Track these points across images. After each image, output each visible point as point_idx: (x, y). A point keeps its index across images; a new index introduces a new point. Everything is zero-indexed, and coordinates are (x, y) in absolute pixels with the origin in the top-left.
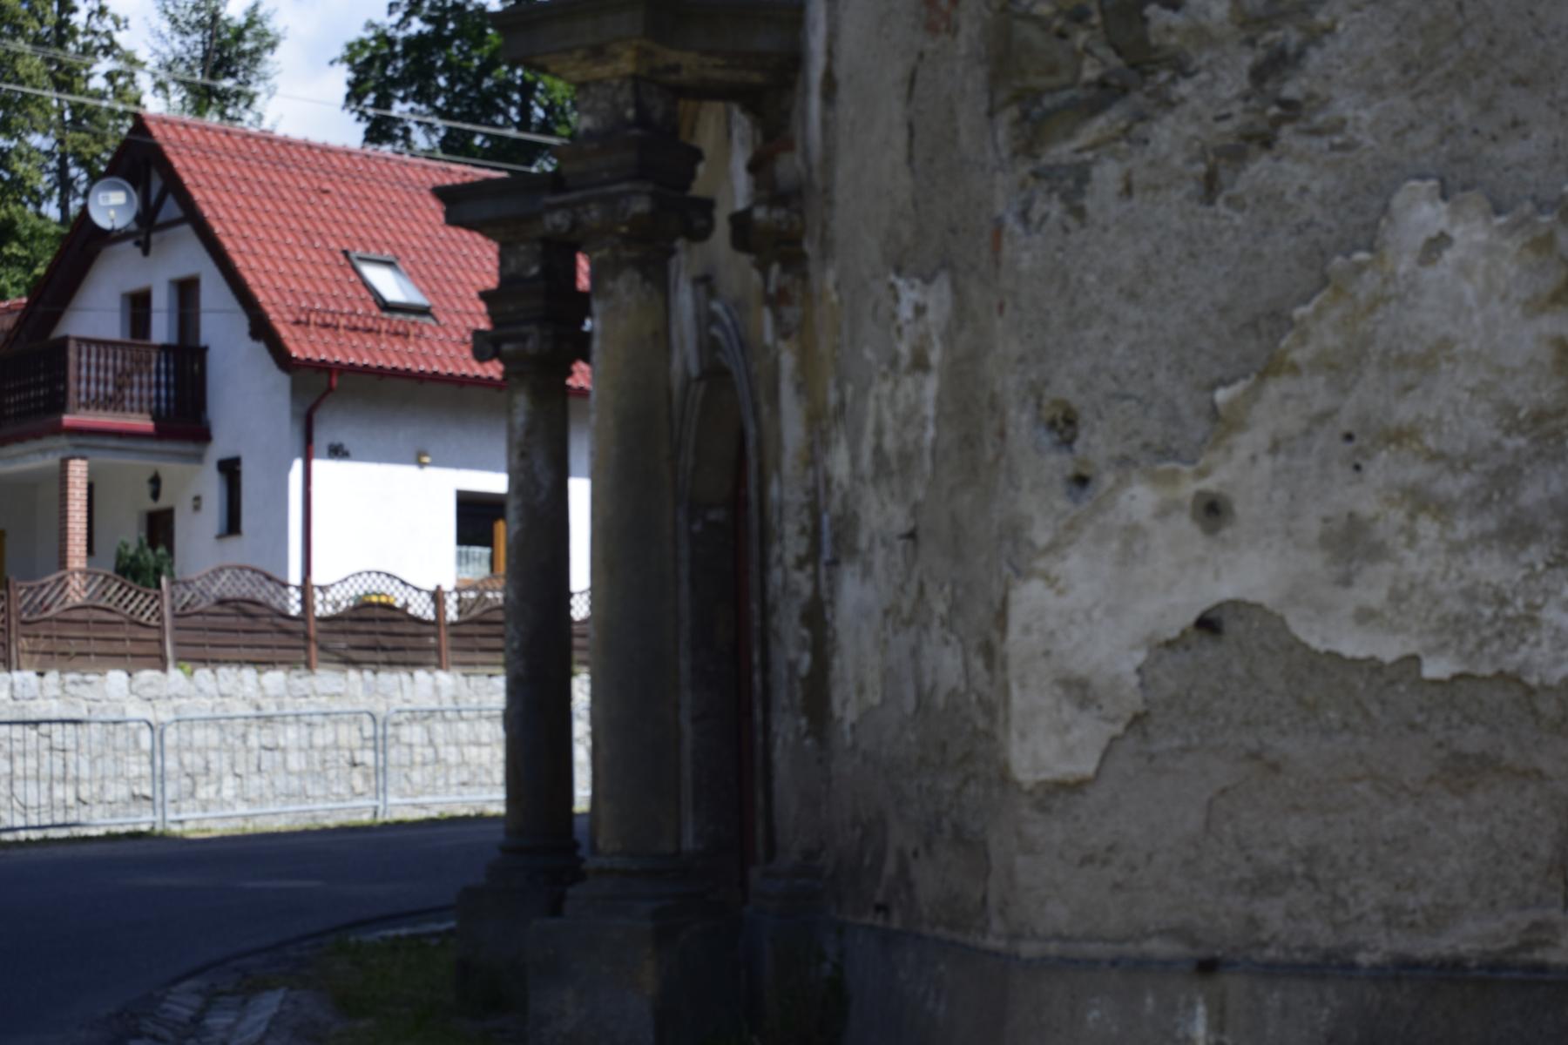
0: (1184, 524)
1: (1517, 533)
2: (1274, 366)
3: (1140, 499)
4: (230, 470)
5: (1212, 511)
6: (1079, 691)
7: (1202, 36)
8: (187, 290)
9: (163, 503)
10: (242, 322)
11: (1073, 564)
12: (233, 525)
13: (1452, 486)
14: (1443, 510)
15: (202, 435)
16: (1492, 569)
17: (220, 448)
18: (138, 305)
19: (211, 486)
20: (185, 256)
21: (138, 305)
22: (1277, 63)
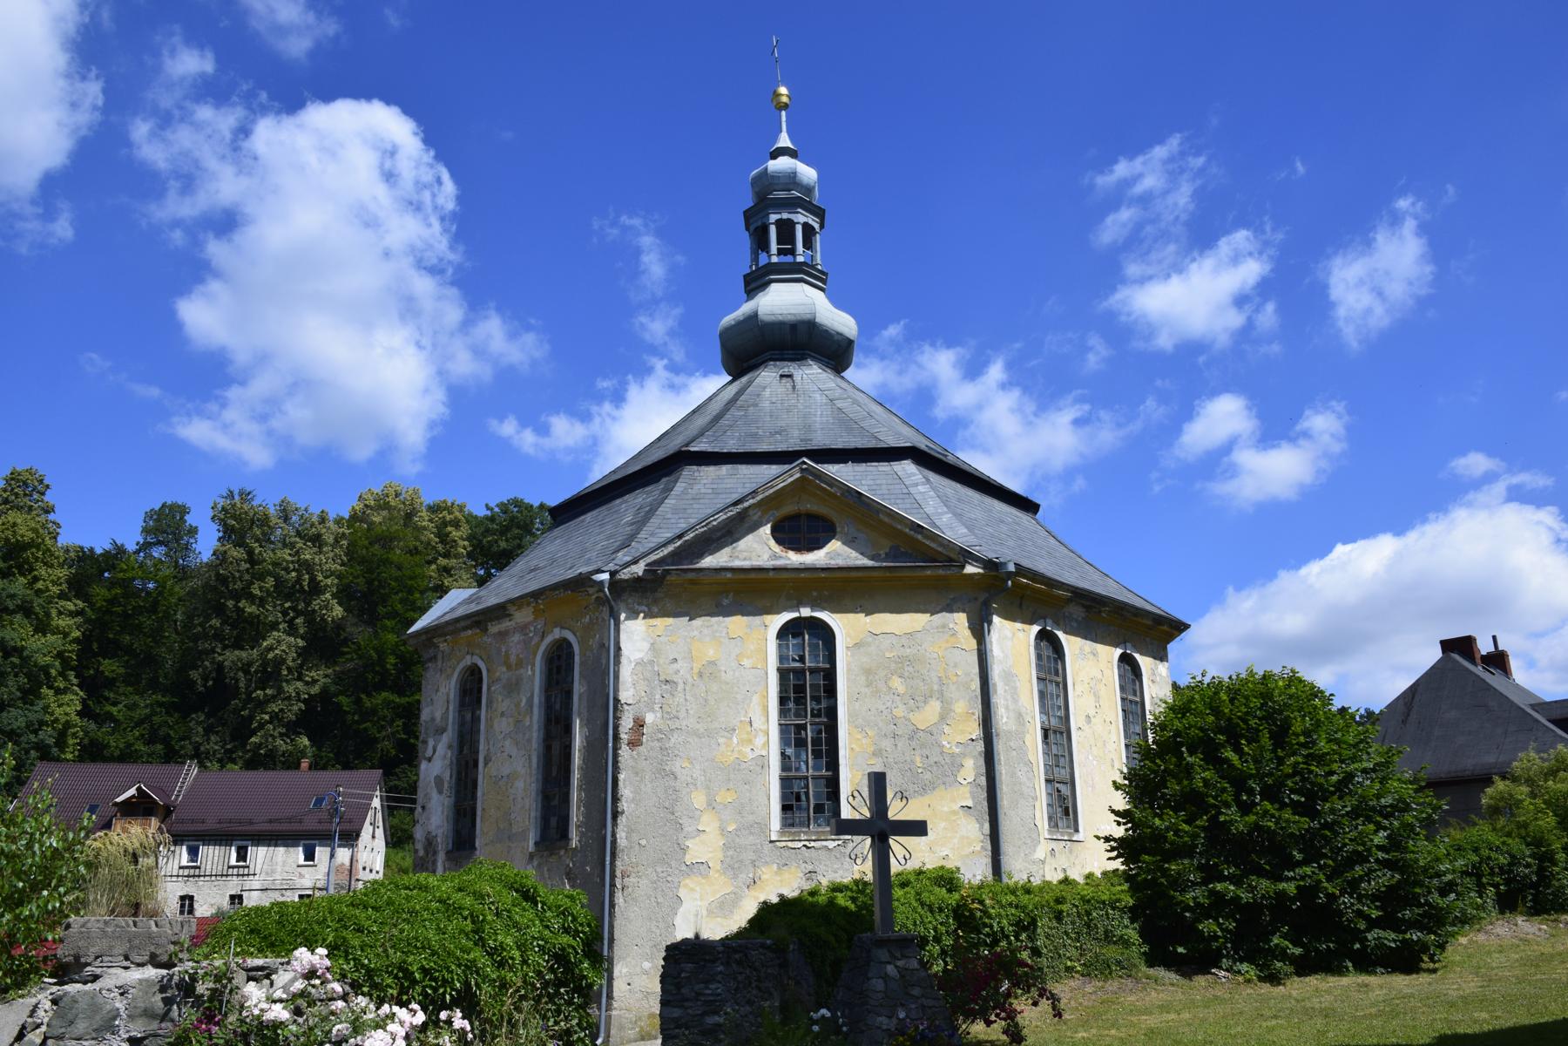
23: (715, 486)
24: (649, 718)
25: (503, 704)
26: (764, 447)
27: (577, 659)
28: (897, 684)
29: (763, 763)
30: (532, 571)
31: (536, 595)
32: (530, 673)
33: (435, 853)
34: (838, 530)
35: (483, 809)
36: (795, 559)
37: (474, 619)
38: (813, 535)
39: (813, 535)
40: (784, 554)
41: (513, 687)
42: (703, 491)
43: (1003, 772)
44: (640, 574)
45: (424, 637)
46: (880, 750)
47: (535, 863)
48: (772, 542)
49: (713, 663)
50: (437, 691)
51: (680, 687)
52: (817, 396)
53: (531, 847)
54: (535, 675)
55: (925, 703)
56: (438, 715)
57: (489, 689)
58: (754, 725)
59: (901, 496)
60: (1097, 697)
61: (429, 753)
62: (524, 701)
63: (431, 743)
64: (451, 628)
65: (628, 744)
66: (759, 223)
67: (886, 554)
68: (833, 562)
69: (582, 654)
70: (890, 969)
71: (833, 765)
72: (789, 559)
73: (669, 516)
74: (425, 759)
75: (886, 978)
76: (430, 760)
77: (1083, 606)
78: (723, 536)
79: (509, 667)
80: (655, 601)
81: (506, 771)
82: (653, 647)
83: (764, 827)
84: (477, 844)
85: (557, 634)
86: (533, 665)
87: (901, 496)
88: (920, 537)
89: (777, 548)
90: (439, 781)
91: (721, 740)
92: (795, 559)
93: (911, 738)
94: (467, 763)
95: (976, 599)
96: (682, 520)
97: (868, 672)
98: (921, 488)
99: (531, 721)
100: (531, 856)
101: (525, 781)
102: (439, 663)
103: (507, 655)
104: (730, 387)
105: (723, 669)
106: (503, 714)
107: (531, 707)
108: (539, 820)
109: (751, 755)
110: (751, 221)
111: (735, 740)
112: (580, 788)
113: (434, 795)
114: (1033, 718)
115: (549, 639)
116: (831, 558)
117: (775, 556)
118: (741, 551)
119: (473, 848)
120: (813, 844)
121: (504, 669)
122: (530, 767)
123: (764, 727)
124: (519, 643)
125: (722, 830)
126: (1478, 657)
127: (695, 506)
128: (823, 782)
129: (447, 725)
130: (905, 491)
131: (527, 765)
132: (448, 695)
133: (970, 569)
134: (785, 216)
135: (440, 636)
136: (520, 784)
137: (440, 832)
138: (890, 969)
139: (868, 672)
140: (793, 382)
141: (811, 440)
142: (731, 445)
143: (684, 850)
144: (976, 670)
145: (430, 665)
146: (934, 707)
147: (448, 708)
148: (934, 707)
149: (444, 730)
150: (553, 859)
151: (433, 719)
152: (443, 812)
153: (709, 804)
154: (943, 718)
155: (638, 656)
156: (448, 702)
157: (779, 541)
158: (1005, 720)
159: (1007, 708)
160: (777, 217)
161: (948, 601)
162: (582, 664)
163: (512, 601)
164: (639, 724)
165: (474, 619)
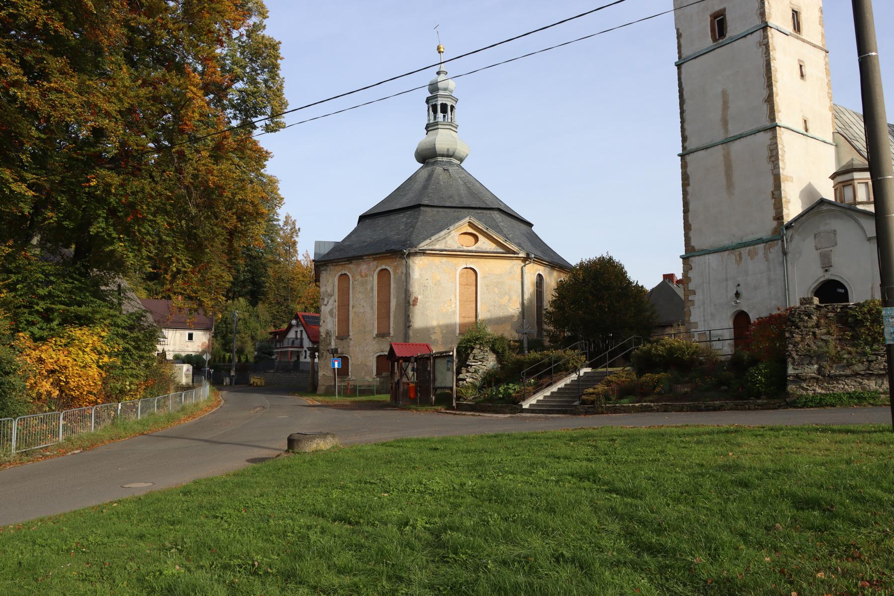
8: (302, 331)
18: (297, 332)
20: (302, 328)
21: (297, 332)
24: (419, 297)
26: (448, 204)
27: (392, 276)
28: (496, 290)
31: (376, 254)
33: (330, 336)
41: (363, 284)
49: (439, 281)
51: (429, 288)
53: (375, 336)
55: (504, 296)
57: (353, 282)
61: (326, 302)
63: (326, 300)
66: (434, 103)
69: (394, 275)
76: (326, 305)
78: (443, 239)
79: (362, 276)
80: (421, 260)
81: (362, 310)
85: (384, 267)
90: (331, 312)
93: (499, 307)
97: (487, 286)
98: (502, 224)
99: (373, 294)
102: (329, 273)
103: (361, 271)
104: (423, 171)
106: (360, 292)
107: (373, 291)
109: (451, 310)
110: (430, 101)
112: (395, 317)
115: (380, 268)
121: (360, 277)
122: (372, 308)
124: (366, 268)
125: (441, 332)
126: (675, 281)
133: (520, 255)
134: (444, 102)
139: (487, 286)
141: (463, 202)
142: (436, 203)
143: (431, 338)
144: (520, 287)
146: (507, 297)
147: (334, 288)
148: (507, 297)
149: (332, 296)
151: (327, 291)
154: (509, 300)
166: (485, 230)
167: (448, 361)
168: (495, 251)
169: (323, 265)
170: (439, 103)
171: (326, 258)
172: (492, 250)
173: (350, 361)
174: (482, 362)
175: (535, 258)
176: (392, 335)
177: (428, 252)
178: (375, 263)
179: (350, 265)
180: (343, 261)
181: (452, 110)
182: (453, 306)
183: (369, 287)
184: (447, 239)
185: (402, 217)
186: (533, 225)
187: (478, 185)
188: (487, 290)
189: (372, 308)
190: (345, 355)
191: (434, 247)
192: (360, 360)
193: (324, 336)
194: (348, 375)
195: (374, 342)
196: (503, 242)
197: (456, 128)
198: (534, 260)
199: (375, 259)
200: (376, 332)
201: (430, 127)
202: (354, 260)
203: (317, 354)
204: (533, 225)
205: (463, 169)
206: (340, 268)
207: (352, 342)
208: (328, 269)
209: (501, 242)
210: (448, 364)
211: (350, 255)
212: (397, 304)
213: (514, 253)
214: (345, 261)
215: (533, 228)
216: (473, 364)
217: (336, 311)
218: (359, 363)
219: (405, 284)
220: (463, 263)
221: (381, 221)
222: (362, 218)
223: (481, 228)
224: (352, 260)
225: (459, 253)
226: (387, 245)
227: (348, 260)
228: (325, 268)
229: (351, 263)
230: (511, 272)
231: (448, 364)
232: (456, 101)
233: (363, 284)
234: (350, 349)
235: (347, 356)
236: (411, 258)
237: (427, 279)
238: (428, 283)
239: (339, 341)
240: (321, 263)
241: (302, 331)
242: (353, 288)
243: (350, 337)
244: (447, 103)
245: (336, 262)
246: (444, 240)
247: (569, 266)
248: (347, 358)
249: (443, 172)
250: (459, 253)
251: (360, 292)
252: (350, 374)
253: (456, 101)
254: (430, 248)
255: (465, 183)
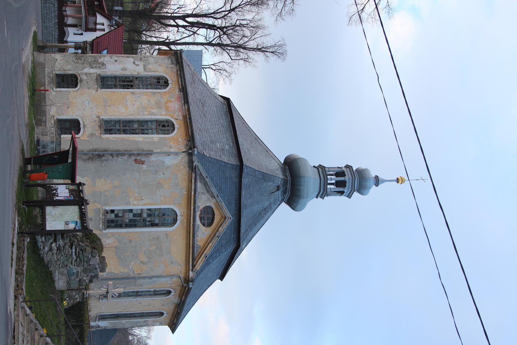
0: (60, 59)
1: (60, 68)
2: (66, 62)
3: (62, 58)
4: (82, 34)
5: (61, 60)
6: (55, 56)
7: (78, 61)
8: (104, 30)
9: (78, 26)
10: (98, 36)
11: (59, 56)
12: (75, 34)
13: (61, 67)
14: (61, 66)
15: (86, 31)
16: (59, 67)
17: (84, 33)
18: (103, 24)
19: (80, 32)
20: (107, 30)
21: (103, 24)
22: (77, 63)
23: (229, 178)
24: (144, 166)
25: (153, 100)
26: (243, 193)
27: (166, 136)
28: (153, 248)
29: (128, 204)
30: (202, 104)
31: (190, 119)
32: (164, 113)
34: (207, 228)
35: (115, 92)
36: (198, 214)
37: (185, 88)
38: (206, 219)
39: (206, 219)
40: (199, 210)
41: (158, 105)
42: (227, 174)
43: (123, 281)
44: (194, 164)
45: (180, 61)
46: (131, 242)
47: (96, 119)
48: (204, 206)
50: (160, 66)
52: (268, 203)
53: (101, 117)
54: (162, 116)
56: (150, 67)
57: (159, 93)
58: (141, 201)
59: (221, 244)
60: (149, 306)
61: (137, 63)
62: (153, 111)
64: (182, 75)
65: (136, 159)
67: (198, 244)
68: (196, 226)
70: (77, 296)
71: (127, 226)
72: (198, 212)
73: (217, 165)
74: (134, 60)
75: (75, 295)
76: (134, 63)
77: (180, 303)
78: (207, 190)
79: (166, 103)
82: (169, 167)
83: (106, 204)
84: (102, 89)
85: (176, 126)
86: (166, 115)
87: (221, 244)
88: (203, 256)
89: (201, 208)
91: (136, 190)
92: (198, 214)
94: (131, 82)
95: (181, 273)
96: (215, 170)
97: (158, 238)
100: (98, 117)
101: (125, 112)
102: (170, 66)
103: (171, 101)
105: (161, 190)
106: (149, 100)
107: (151, 115)
108: (111, 119)
109: (131, 200)
110: (348, 169)
111: (136, 195)
113: (121, 66)
114: (141, 289)
116: (197, 226)
117: (199, 207)
118: (201, 196)
119: (102, 88)
120: (101, 220)
121: (166, 100)
123: (140, 204)
125: (106, 191)
127: (221, 173)
128: (121, 223)
129: (146, 72)
130: (223, 245)
131: (130, 113)
132: (158, 71)
133: (191, 273)
134: (347, 184)
135: (180, 68)
136: (123, 110)
137: (107, 70)
138: (77, 296)
139: (158, 238)
140: (276, 192)
145: (170, 61)
147: (153, 71)
148: (146, 260)
150: (97, 128)
151: (149, 64)
152: (114, 71)
153: (115, 187)
154: (142, 262)
155: (166, 162)
156: (155, 71)
157: (204, 208)
158: (140, 281)
159: (144, 282)
160: (347, 181)
161: (180, 264)
162: (165, 138)
163: (189, 108)
164: (143, 163)
165: (185, 88)
166: (217, 235)
167: (77, 222)
168: (195, 245)
169: (177, 60)
170: (346, 178)
171: (184, 64)
172: (196, 243)
173: (74, 89)
174: (76, 260)
175: (189, 288)
176: (102, 136)
177: (194, 175)
178: (181, 118)
179: (178, 90)
180: (182, 81)
181: (339, 192)
182: (136, 203)
183: (154, 111)
184: (207, 194)
185: (229, 145)
186: (222, 280)
187: (262, 222)
188: (154, 239)
189: (131, 115)
190: (79, 84)
191: (198, 181)
192: (75, 101)
193: (100, 60)
194: (57, 87)
195: (94, 116)
196: (204, 254)
197: (321, 197)
198: (186, 287)
199: (185, 117)
200: (106, 117)
201: (321, 169)
202: (184, 94)
203: (80, 51)
204: (222, 280)
205: (279, 205)
206: (175, 78)
207: (94, 92)
208: (173, 66)
209: (205, 252)
210: (72, 222)
211: (189, 89)
212: (136, 142)
213: (193, 266)
214: (182, 84)
215: (218, 281)
216: (74, 250)
217: (127, 73)
218: (70, 100)
219: (159, 150)
220: (180, 211)
221: (224, 121)
222: (227, 100)
223: (220, 229)
224: (183, 92)
225: (192, 208)
226: (200, 130)
227: (183, 88)
228: (174, 62)
229: (180, 91)
230: (172, 263)
231: (72, 222)
232: (349, 196)
233: (158, 105)
234: (86, 90)
235: (79, 86)
236: (187, 157)
237: (164, 174)
238: (160, 175)
239: (95, 77)
240: (179, 58)
241: (104, 30)
242: (154, 93)
243: (99, 90)
244: (347, 187)
245: (180, 73)
246: (205, 191)
247: (180, 321)
248: (76, 86)
249: (276, 185)
250: (192, 208)
251: (149, 100)
252: (58, 89)
253: (349, 196)
254: (198, 177)
255: (265, 209)
